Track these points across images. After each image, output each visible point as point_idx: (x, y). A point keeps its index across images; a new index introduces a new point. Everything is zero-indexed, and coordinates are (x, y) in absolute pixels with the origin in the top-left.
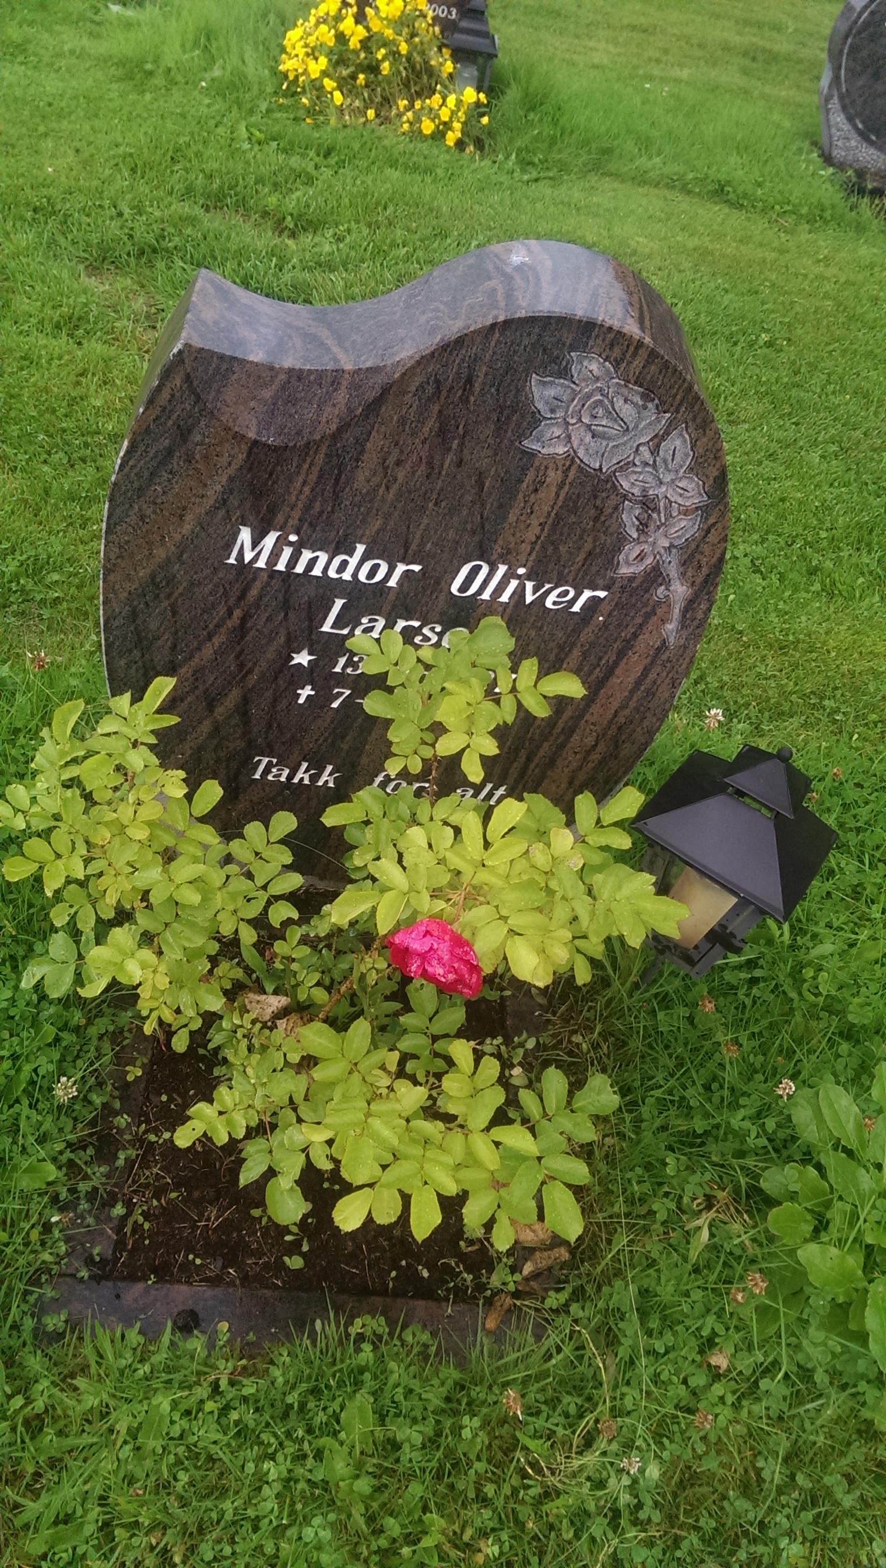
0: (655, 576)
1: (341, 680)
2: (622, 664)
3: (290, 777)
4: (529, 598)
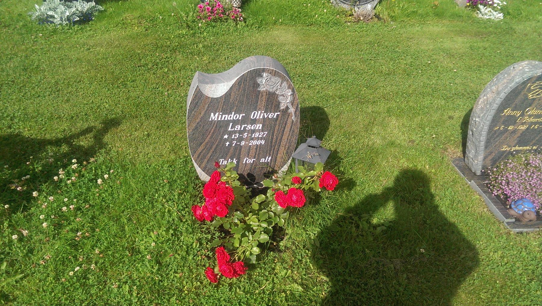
0: (287, 108)
1: (234, 139)
4: (266, 117)
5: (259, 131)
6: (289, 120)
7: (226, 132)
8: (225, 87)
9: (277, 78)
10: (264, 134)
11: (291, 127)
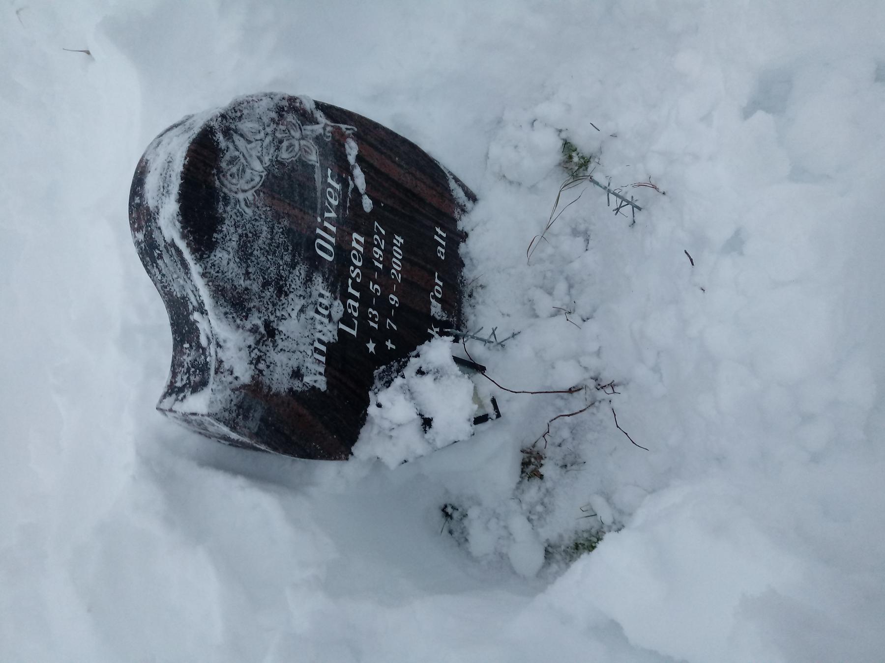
1: (382, 324)
2: (368, 159)
4: (333, 215)
11: (371, 145)
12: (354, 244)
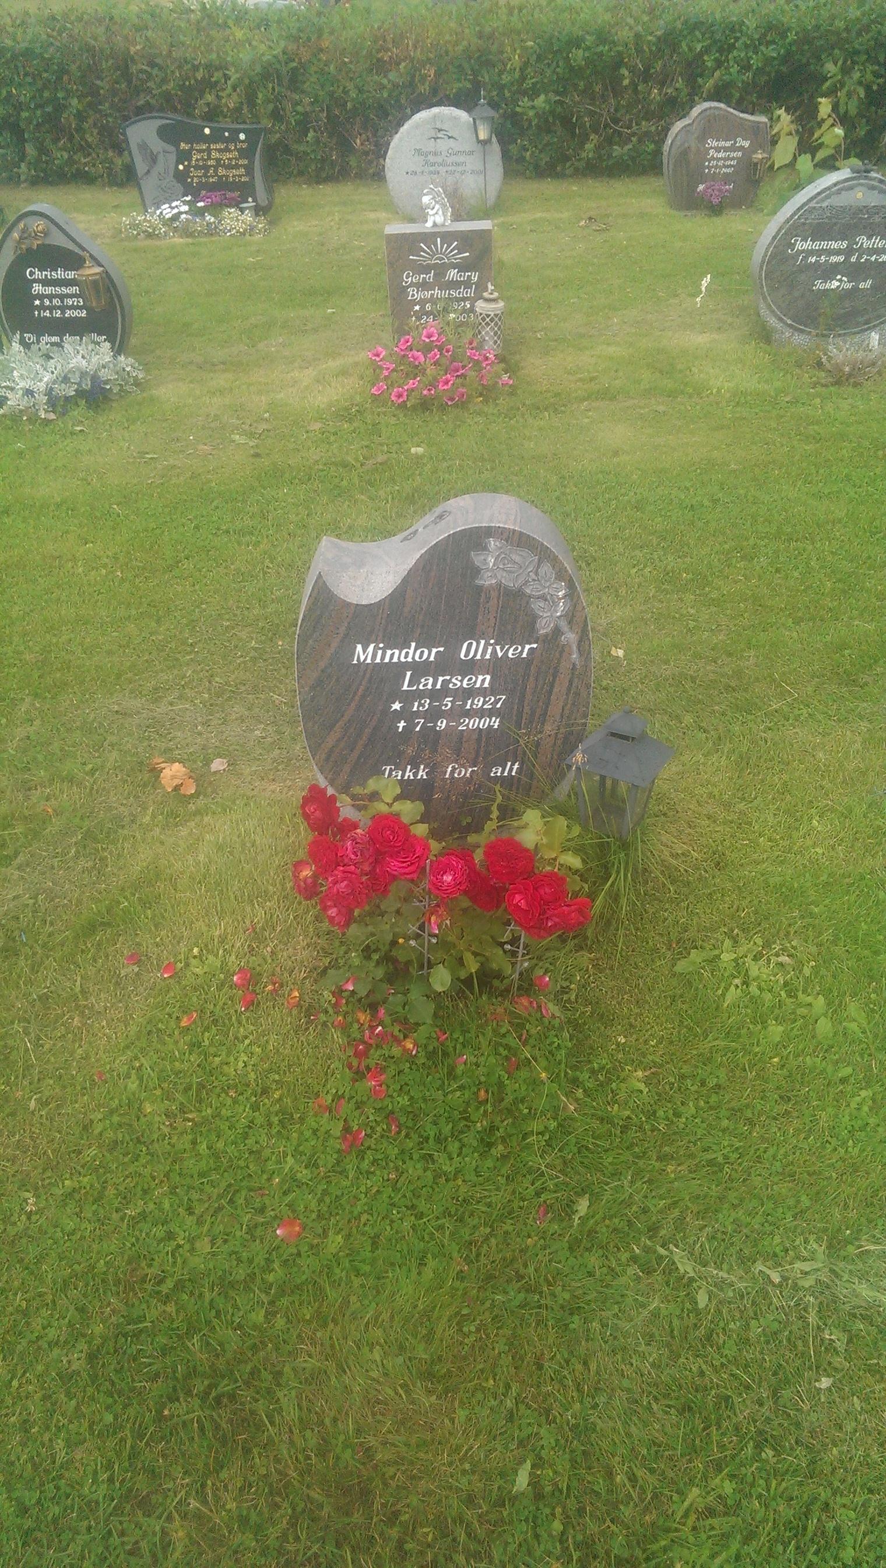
0: (557, 632)
2: (557, 681)
3: (403, 776)
4: (500, 655)
5: (483, 692)
6: (563, 664)
7: (397, 694)
8: (391, 578)
9: (525, 552)
10: (497, 702)
11: (571, 682)
12: (481, 678)
